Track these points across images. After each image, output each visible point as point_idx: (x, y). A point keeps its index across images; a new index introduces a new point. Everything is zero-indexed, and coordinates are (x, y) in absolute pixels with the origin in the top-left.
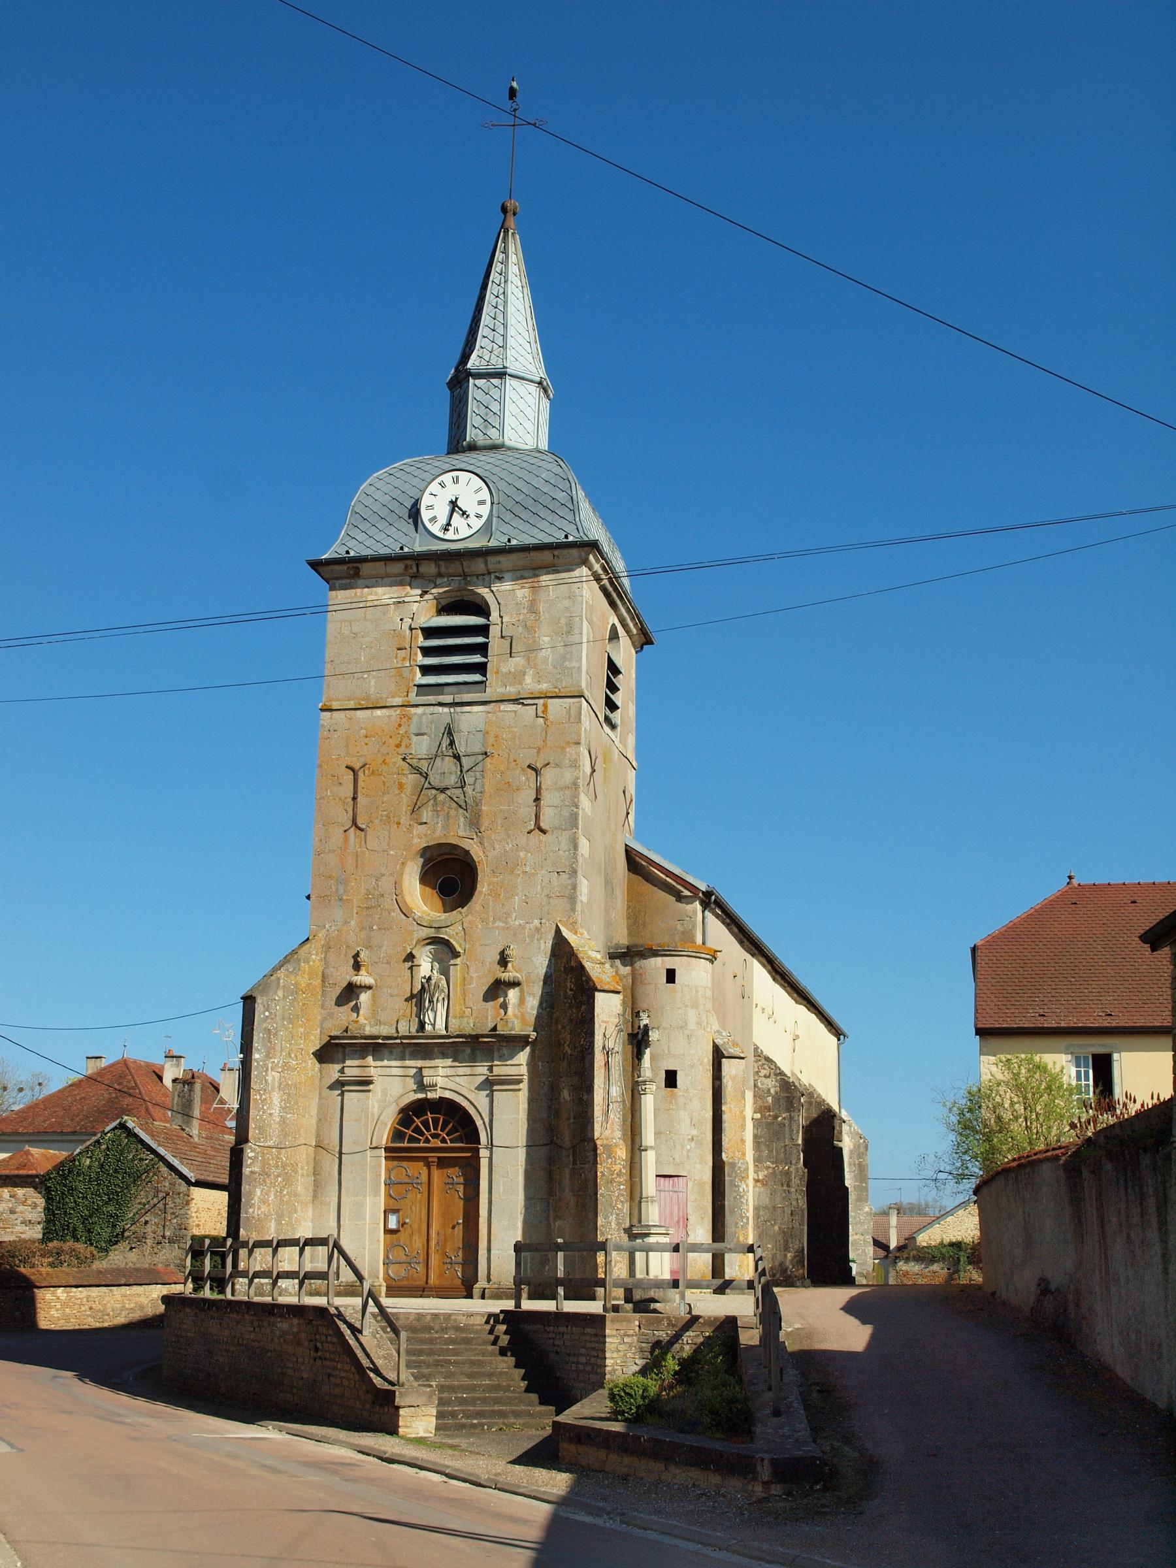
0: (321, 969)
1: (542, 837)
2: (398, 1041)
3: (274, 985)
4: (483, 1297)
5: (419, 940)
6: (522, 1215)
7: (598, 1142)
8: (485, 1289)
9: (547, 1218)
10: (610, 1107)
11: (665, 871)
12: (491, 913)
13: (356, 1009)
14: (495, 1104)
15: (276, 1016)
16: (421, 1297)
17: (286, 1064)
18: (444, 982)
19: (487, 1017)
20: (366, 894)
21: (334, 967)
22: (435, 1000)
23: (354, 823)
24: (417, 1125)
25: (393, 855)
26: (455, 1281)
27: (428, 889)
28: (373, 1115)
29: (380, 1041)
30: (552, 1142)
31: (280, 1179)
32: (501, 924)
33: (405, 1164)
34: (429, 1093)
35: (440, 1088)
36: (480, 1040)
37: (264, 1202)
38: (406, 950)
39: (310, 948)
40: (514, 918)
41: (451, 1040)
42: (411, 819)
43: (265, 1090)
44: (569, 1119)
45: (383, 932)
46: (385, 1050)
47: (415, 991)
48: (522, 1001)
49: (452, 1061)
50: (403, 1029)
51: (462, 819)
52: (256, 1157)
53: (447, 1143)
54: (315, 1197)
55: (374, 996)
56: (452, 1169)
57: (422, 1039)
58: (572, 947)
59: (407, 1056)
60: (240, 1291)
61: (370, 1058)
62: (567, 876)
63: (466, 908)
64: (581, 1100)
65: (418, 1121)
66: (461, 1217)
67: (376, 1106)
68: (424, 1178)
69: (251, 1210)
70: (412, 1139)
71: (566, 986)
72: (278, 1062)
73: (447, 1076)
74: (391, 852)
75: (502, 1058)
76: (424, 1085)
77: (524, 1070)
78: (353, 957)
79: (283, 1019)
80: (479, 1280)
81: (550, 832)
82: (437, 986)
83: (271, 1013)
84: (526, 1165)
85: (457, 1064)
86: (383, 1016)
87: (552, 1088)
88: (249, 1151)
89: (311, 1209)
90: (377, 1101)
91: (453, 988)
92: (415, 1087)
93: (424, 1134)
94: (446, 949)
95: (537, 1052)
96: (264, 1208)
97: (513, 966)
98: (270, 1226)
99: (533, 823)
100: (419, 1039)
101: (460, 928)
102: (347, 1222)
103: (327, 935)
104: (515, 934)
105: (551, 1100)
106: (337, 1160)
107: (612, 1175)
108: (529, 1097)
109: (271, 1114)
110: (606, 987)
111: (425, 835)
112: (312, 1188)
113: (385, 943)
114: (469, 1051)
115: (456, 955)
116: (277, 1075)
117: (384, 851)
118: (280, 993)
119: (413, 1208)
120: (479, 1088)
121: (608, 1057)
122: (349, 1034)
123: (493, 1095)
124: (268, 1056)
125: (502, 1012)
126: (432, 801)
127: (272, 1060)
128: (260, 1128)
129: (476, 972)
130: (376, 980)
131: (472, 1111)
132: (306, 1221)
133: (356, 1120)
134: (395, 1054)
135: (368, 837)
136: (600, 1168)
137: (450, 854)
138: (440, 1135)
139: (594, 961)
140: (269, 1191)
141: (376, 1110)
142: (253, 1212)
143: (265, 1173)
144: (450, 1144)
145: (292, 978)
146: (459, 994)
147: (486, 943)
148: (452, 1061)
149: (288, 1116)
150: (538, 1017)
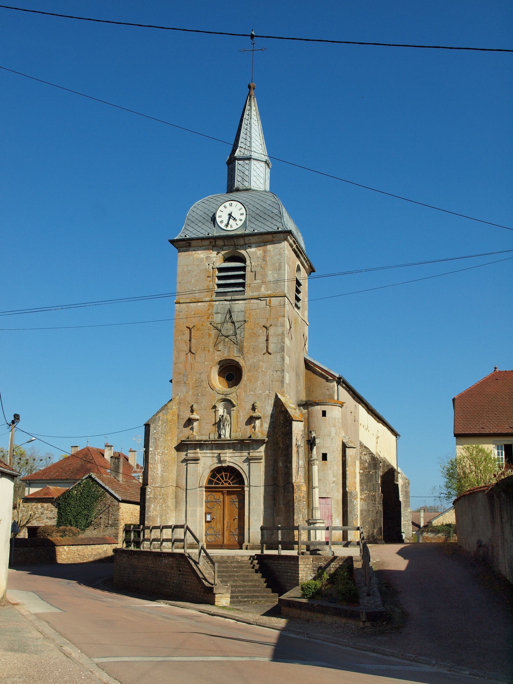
0: (177, 412)
1: (270, 356)
2: (210, 442)
3: (157, 420)
4: (247, 549)
7: (294, 484)
8: (247, 545)
9: (273, 516)
10: (299, 469)
11: (321, 369)
12: (248, 388)
13: (192, 429)
16: (221, 549)
17: (163, 452)
18: (229, 417)
19: (247, 432)
20: (196, 381)
21: (182, 411)
22: (225, 425)
23: (190, 351)
24: (218, 477)
27: (222, 378)
28: (200, 473)
29: (202, 442)
30: (275, 484)
31: (161, 500)
33: (213, 494)
34: (223, 464)
35: (228, 462)
36: (244, 441)
39: (173, 403)
40: (258, 390)
41: (232, 442)
42: (214, 349)
43: (155, 463)
44: (282, 474)
46: (204, 446)
47: (217, 422)
48: (262, 425)
49: (233, 451)
50: (212, 437)
51: (235, 349)
52: (151, 491)
53: (231, 485)
54: (176, 507)
55: (199, 423)
58: (283, 403)
59: (214, 448)
60: (146, 547)
61: (198, 450)
62: (280, 372)
63: (238, 386)
64: (287, 466)
66: (237, 516)
67: (201, 470)
68: (222, 499)
69: (149, 513)
70: (216, 483)
72: (160, 451)
73: (230, 457)
74: (206, 363)
75: (253, 449)
76: (221, 461)
77: (263, 454)
78: (191, 407)
79: (162, 433)
81: (273, 354)
83: (156, 431)
84: (264, 494)
85: (235, 452)
86: (203, 432)
87: (275, 462)
88: (148, 489)
89: (174, 512)
90: (201, 467)
92: (217, 461)
93: (221, 481)
94: (229, 403)
95: (268, 446)
96: (155, 513)
99: (265, 350)
100: (219, 441)
101: (235, 395)
102: (190, 518)
103: (179, 398)
104: (259, 397)
105: (275, 466)
106: (185, 492)
107: (300, 498)
109: (157, 473)
110: (297, 419)
111: (220, 356)
112: (174, 504)
114: (240, 446)
115: (234, 406)
116: (159, 457)
117: (203, 362)
118: (160, 422)
119: (217, 512)
120: (244, 462)
121: (298, 449)
122: (189, 439)
124: (156, 449)
125: (253, 430)
126: (223, 341)
127: (157, 451)
128: (153, 479)
129: (242, 413)
130: (200, 417)
132: (172, 517)
133: (193, 475)
134: (209, 447)
135: (196, 356)
136: (295, 495)
138: (228, 481)
139: (292, 408)
140: (157, 505)
141: (201, 471)
143: (155, 498)
144: (232, 485)
145: (165, 416)
146: (235, 422)
147: (246, 401)
148: (233, 451)
150: (269, 432)
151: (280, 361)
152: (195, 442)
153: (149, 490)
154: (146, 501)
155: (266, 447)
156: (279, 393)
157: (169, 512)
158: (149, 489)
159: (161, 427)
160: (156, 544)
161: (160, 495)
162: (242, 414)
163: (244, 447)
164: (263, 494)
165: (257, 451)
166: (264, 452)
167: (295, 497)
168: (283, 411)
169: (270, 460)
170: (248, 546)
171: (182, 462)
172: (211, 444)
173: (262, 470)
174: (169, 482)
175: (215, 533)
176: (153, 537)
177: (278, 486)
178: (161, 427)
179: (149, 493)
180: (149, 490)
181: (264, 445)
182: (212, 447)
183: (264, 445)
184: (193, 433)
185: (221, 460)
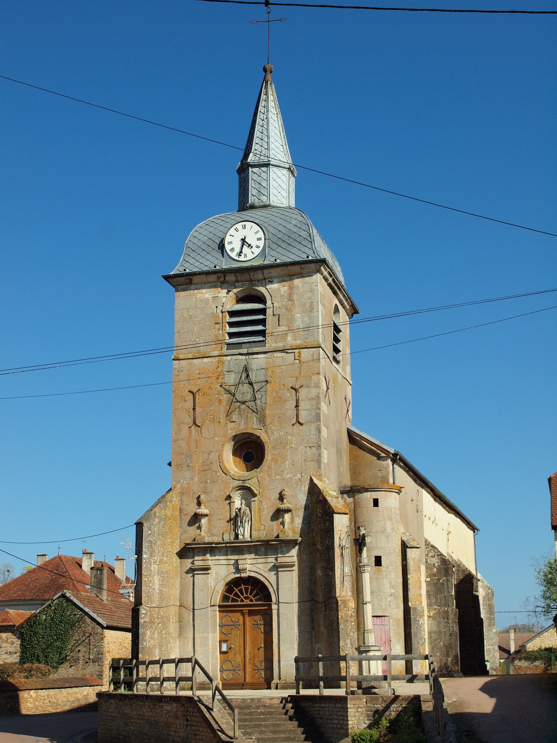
0: (179, 506)
1: (301, 427)
2: (224, 545)
3: (153, 516)
4: (277, 688)
5: (233, 487)
6: (298, 641)
7: (339, 599)
8: (278, 684)
9: (312, 643)
10: (345, 579)
12: (273, 471)
13: (199, 528)
14: (280, 579)
15: (155, 533)
16: (242, 689)
17: (161, 560)
18: (248, 511)
19: (273, 530)
21: (186, 505)
22: (244, 521)
23: (195, 423)
24: (236, 592)
25: (217, 440)
26: (261, 680)
27: (237, 459)
28: (211, 587)
29: (214, 545)
30: (312, 599)
31: (160, 625)
32: (280, 477)
33: (230, 614)
34: (242, 574)
35: (249, 571)
37: (151, 638)
38: (226, 493)
39: (172, 494)
40: (286, 473)
42: (226, 420)
43: (150, 575)
44: (321, 586)
45: (213, 484)
46: (217, 550)
47: (232, 517)
48: (292, 520)
49: (255, 555)
50: (226, 538)
51: (255, 419)
52: (146, 613)
53: (253, 602)
55: (209, 521)
56: (256, 616)
57: (238, 543)
58: (320, 489)
60: (140, 689)
61: (208, 555)
63: (259, 469)
64: (328, 575)
65: (236, 590)
66: (263, 643)
67: (213, 582)
68: (241, 622)
69: (145, 643)
70: (233, 600)
71: (317, 511)
72: (157, 559)
73: (252, 564)
74: (216, 439)
75: (282, 553)
76: (239, 569)
77: (295, 559)
78: (197, 498)
79: (159, 535)
80: (274, 679)
82: (244, 513)
83: (152, 532)
84: (298, 613)
85: (257, 557)
86: (214, 531)
87: (311, 569)
88: (142, 610)
89: (178, 641)
91: (254, 514)
93: (240, 597)
95: (302, 548)
96: (152, 642)
97: (287, 501)
98: (156, 652)
99: (295, 419)
100: (236, 543)
101: (256, 480)
102: (199, 648)
103: (181, 486)
104: (287, 483)
106: (192, 613)
108: (298, 574)
109: (154, 589)
110: (340, 511)
111: (235, 428)
112: (178, 629)
113: (215, 490)
114: (264, 549)
115: (255, 495)
116: (156, 566)
117: (212, 438)
118: (157, 520)
119: (236, 639)
120: (271, 570)
121: (342, 551)
122: (196, 542)
123: (278, 574)
124: (151, 556)
125: (282, 527)
126: (238, 409)
127: (153, 558)
128: (148, 597)
129: (266, 505)
130: (210, 511)
131: (267, 583)
132: (176, 648)
133: (202, 590)
135: (203, 430)
137: (248, 438)
138: (249, 597)
139: (332, 497)
140: (155, 632)
141: (213, 584)
142: (146, 644)
143: (152, 622)
144: (255, 602)
145: (163, 511)
146: (257, 517)
147: (271, 488)
148: (255, 555)
149: (164, 589)
150: (302, 529)
151: (314, 433)
152: (204, 546)
153: (144, 612)
154: (140, 627)
155: (300, 549)
156: (315, 477)
157: (171, 641)
158: (144, 610)
159: (157, 526)
160: (155, 685)
161: (159, 618)
162: (266, 507)
163: (269, 550)
164: (297, 613)
165: (287, 555)
166: (297, 556)
167: (340, 617)
168: (320, 501)
169: (306, 567)
170: (278, 684)
171: (187, 572)
172: (226, 548)
173: (294, 581)
174: (170, 600)
175: (234, 667)
176: (150, 676)
177: (318, 602)
178: (157, 526)
179: (143, 616)
180: (144, 612)
181: (297, 547)
182: (227, 551)
183: (297, 547)
184: (201, 533)
185: (240, 568)
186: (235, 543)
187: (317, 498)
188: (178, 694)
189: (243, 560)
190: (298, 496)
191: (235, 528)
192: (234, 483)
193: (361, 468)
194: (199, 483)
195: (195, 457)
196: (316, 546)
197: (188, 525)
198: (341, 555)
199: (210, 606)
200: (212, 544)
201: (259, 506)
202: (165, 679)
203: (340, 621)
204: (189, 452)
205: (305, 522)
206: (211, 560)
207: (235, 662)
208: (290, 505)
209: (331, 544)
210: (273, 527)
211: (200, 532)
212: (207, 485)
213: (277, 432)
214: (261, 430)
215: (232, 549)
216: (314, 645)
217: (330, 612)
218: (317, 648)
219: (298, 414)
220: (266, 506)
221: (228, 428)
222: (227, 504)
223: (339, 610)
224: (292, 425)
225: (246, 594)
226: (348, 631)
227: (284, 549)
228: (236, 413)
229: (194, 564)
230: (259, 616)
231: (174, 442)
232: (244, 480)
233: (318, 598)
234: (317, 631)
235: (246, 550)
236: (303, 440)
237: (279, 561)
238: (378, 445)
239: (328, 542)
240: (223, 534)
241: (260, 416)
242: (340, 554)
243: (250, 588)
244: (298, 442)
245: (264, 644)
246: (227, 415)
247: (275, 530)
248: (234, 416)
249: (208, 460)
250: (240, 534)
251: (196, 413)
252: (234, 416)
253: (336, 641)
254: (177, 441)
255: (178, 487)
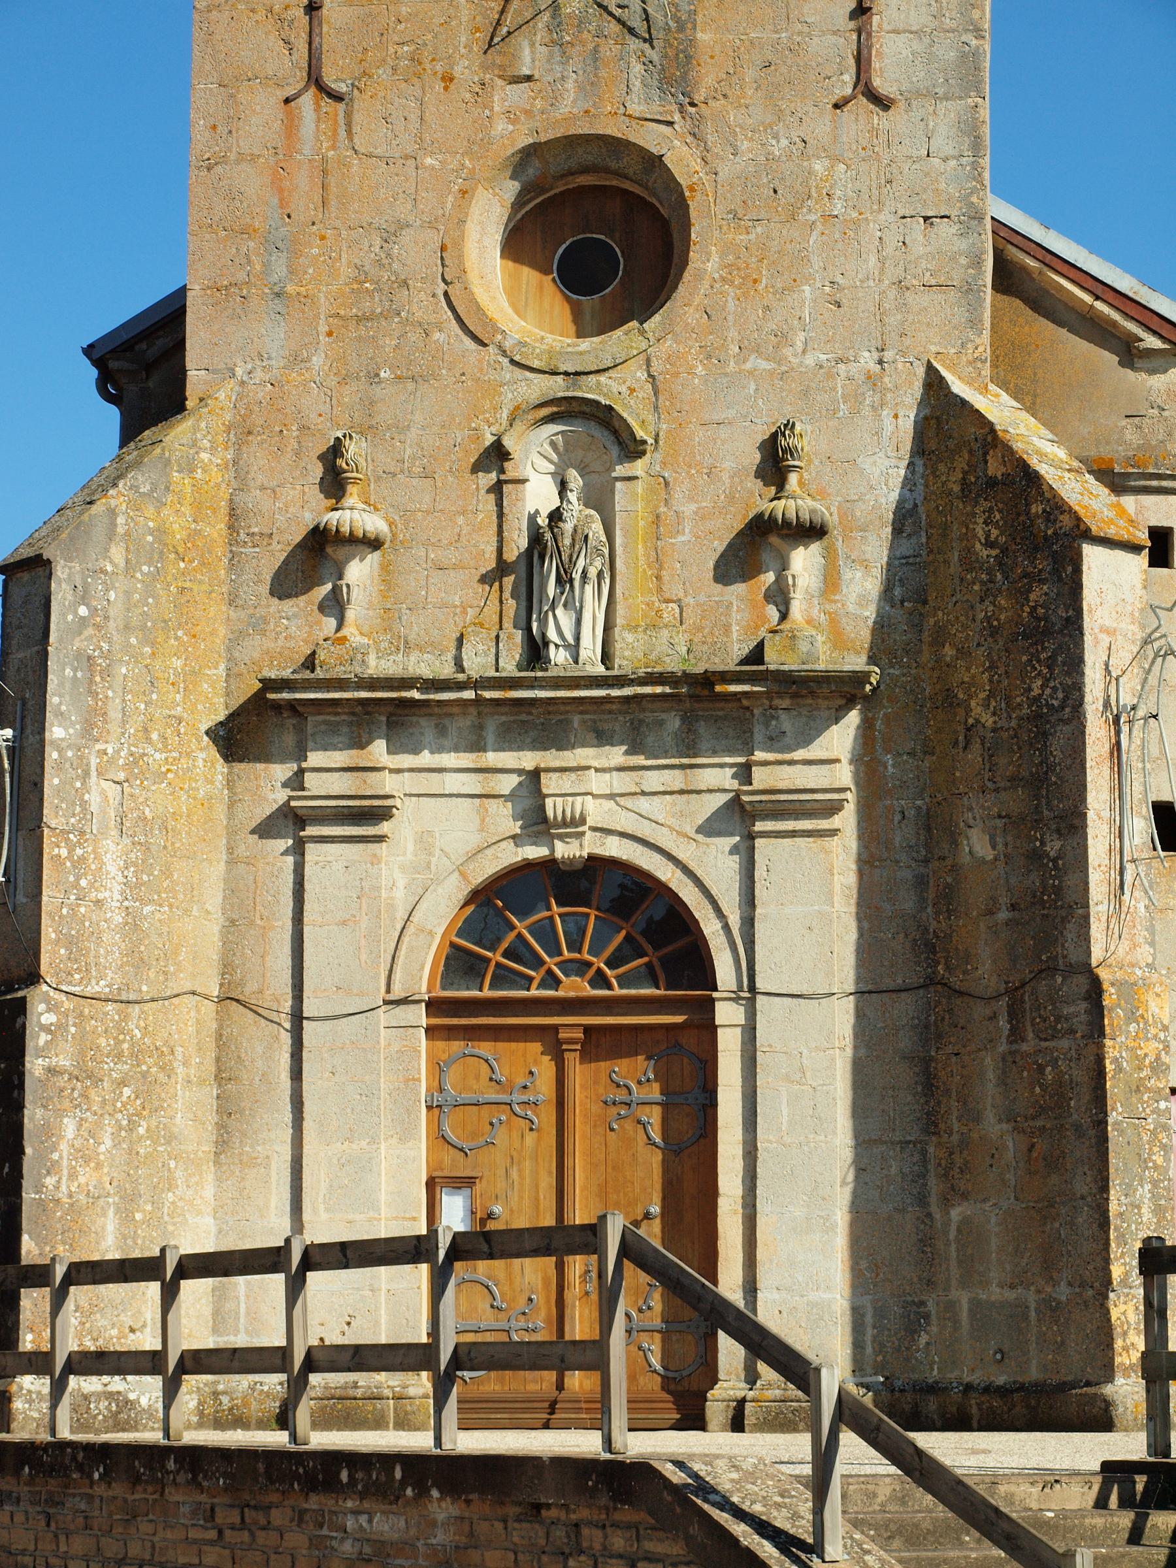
0: (225, 493)
1: (880, 119)
2: (469, 694)
3: (99, 532)
4: (737, 1424)
5: (517, 408)
6: (848, 1190)
7: (1104, 974)
8: (742, 1402)
9: (922, 1200)
10: (1128, 878)
11: (1089, 284)
12: (733, 334)
13: (336, 605)
14: (760, 873)
15: (106, 618)
16: (546, 1426)
17: (136, 760)
18: (596, 529)
19: (727, 629)
20: (355, 280)
21: (263, 488)
22: (577, 576)
23: (315, 79)
24: (520, 936)
25: (433, 168)
26: (642, 1380)
27: (528, 275)
28: (391, 907)
29: (415, 695)
30: (931, 982)
31: (127, 1091)
32: (764, 365)
33: (485, 1048)
34: (559, 845)
35: (594, 829)
36: (718, 688)
37: (84, 1156)
38: (479, 438)
39: (196, 429)
40: (799, 345)
41: (627, 691)
42: (484, 67)
43: (82, 833)
44: (990, 912)
45: (410, 386)
46: (423, 722)
47: (511, 555)
48: (831, 581)
49: (627, 753)
50: (477, 662)
51: (637, 68)
52: (61, 1027)
53: (609, 987)
54: (223, 1142)
55: (386, 571)
56: (625, 1062)
57: (542, 688)
58: (991, 424)
59: (490, 738)
60: (27, 1418)
61: (379, 746)
62: (954, 229)
63: (657, 318)
64: (1036, 857)
65: (521, 926)
66: (657, 1197)
67: (401, 883)
68: (545, 1086)
69: (50, 1181)
70: (503, 977)
71: (969, 536)
72: (118, 752)
73: (611, 796)
74: (429, 161)
75: (774, 741)
76: (545, 820)
77: (844, 775)
78: (321, 458)
79: (127, 627)
80: (721, 1376)
81: (902, 105)
82: (579, 537)
83: (94, 611)
84: (856, 1048)
85: (640, 760)
86: (414, 626)
87: (928, 829)
88: (42, 1007)
89: (210, 1177)
90: (403, 868)
91: (625, 546)
92: (516, 828)
93: (542, 962)
94: (599, 433)
95: (879, 724)
96: (85, 1176)
97: (801, 483)
98: (103, 1228)
99: (849, 78)
100: (532, 687)
101: (642, 375)
102: (324, 1216)
103: (240, 397)
104: (806, 393)
105: (926, 861)
106: (286, 1039)
107: (1140, 1069)
108: (859, 854)
109: (98, 903)
110: (1111, 532)
111: (528, 113)
112: (212, 1118)
113: (418, 417)
114: (677, 723)
115: (632, 449)
116: (112, 790)
117: (407, 157)
118: (117, 553)
119: (514, 1174)
120: (710, 828)
121: (1118, 733)
122: (319, 673)
123: (752, 849)
124: (89, 731)
125: (773, 613)
126: (546, 17)
127: (99, 746)
128: (70, 942)
129: (691, 499)
130: (391, 524)
131: (688, 894)
132: (199, 1213)
133: (344, 923)
134: (453, 731)
135: (357, 117)
136: (1112, 1050)
137: (585, 170)
138: (589, 965)
139: (1055, 464)
140: (99, 1125)
141: (400, 893)
142: (57, 1188)
143: (87, 1075)
144: (618, 991)
145: (150, 511)
146: (642, 561)
147: (716, 417)
148: (627, 753)
149: (147, 909)
150: (881, 627)
151: (949, 150)
152: (364, 694)
153: (48, 1019)
154: (29, 1097)
155: (866, 729)
156: (951, 368)
157: (179, 1174)
158: (49, 1010)
159: (121, 583)
160: (99, 1396)
161: (119, 1055)
162: (689, 509)
163: (702, 728)
164: (849, 1052)
165: (799, 754)
166: (851, 762)
167: (1109, 1067)
168: (992, 483)
169: (898, 817)
170: (748, 1405)
171: (265, 830)
172: (473, 711)
173: (837, 888)
174: (178, 964)
175: (502, 1315)
176: (71, 1343)
177: (961, 994)
178: (121, 583)
179: (43, 1038)
180: (48, 1019)
181: (853, 717)
182: (481, 727)
183: (853, 717)
184: (345, 632)
185: (550, 813)
186: (532, 684)
187: (972, 467)
188: (447, 1445)
189: (565, 775)
190: (859, 461)
191: (523, 614)
192: (523, 388)
193: (1038, 401)
194: (332, 381)
195: (315, 251)
196: (961, 712)
197: (272, 593)
198: (1112, 754)
199: (386, 1002)
200: (411, 687)
201: (657, 507)
202: (317, 1355)
203: (1114, 1087)
204: (285, 225)
205: (897, 592)
206: (391, 771)
207: (506, 1288)
208: (817, 505)
209: (1060, 695)
210: (728, 615)
211: (339, 628)
212: (378, 391)
213: (751, 140)
214: (670, 124)
215: (504, 718)
216: (934, 1209)
217: (1044, 1044)
218: (953, 1227)
219: (865, 52)
220: (693, 507)
221: (492, 110)
222: (483, 492)
223: (1108, 1030)
224: (836, 106)
225: (574, 946)
226: (1145, 1138)
227: (786, 723)
228: (539, 37)
229: (303, 789)
230: (641, 1058)
231: (204, 173)
232: (577, 374)
233: (965, 972)
234: (955, 1138)
235: (584, 722)
236: (890, 182)
237: (757, 784)
238: (1131, 294)
239: (1043, 687)
240: (460, 641)
241: (666, 56)
242: (1107, 746)
243: (592, 918)
244: (864, 189)
245: (664, 1199)
246: (490, 46)
247: (735, 628)
248: (527, 51)
249: (382, 266)
250: (559, 642)
251: (325, 29)
252: (527, 51)
253: (1083, 1186)
254: (219, 169)
255: (222, 395)
